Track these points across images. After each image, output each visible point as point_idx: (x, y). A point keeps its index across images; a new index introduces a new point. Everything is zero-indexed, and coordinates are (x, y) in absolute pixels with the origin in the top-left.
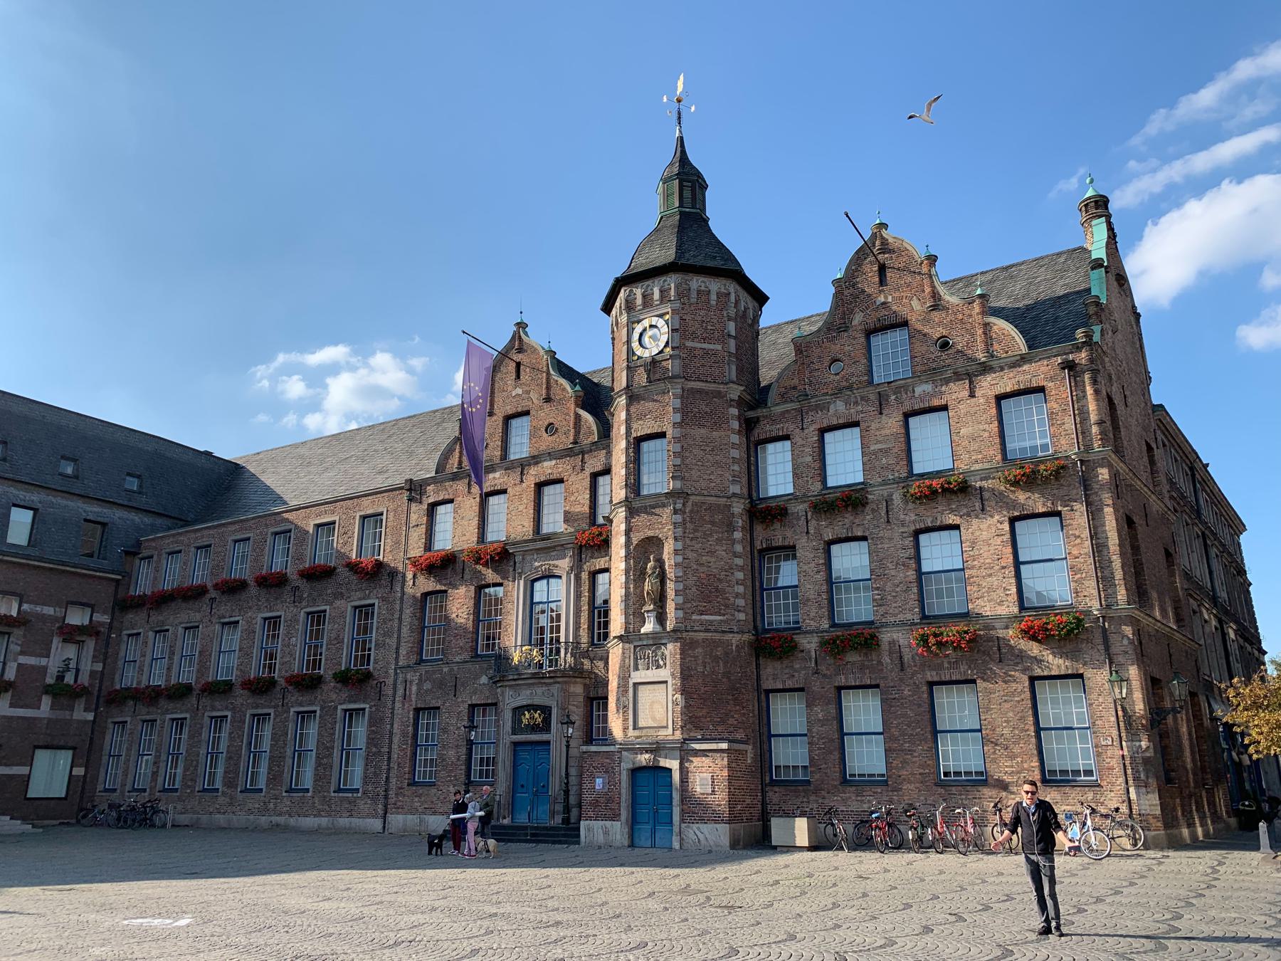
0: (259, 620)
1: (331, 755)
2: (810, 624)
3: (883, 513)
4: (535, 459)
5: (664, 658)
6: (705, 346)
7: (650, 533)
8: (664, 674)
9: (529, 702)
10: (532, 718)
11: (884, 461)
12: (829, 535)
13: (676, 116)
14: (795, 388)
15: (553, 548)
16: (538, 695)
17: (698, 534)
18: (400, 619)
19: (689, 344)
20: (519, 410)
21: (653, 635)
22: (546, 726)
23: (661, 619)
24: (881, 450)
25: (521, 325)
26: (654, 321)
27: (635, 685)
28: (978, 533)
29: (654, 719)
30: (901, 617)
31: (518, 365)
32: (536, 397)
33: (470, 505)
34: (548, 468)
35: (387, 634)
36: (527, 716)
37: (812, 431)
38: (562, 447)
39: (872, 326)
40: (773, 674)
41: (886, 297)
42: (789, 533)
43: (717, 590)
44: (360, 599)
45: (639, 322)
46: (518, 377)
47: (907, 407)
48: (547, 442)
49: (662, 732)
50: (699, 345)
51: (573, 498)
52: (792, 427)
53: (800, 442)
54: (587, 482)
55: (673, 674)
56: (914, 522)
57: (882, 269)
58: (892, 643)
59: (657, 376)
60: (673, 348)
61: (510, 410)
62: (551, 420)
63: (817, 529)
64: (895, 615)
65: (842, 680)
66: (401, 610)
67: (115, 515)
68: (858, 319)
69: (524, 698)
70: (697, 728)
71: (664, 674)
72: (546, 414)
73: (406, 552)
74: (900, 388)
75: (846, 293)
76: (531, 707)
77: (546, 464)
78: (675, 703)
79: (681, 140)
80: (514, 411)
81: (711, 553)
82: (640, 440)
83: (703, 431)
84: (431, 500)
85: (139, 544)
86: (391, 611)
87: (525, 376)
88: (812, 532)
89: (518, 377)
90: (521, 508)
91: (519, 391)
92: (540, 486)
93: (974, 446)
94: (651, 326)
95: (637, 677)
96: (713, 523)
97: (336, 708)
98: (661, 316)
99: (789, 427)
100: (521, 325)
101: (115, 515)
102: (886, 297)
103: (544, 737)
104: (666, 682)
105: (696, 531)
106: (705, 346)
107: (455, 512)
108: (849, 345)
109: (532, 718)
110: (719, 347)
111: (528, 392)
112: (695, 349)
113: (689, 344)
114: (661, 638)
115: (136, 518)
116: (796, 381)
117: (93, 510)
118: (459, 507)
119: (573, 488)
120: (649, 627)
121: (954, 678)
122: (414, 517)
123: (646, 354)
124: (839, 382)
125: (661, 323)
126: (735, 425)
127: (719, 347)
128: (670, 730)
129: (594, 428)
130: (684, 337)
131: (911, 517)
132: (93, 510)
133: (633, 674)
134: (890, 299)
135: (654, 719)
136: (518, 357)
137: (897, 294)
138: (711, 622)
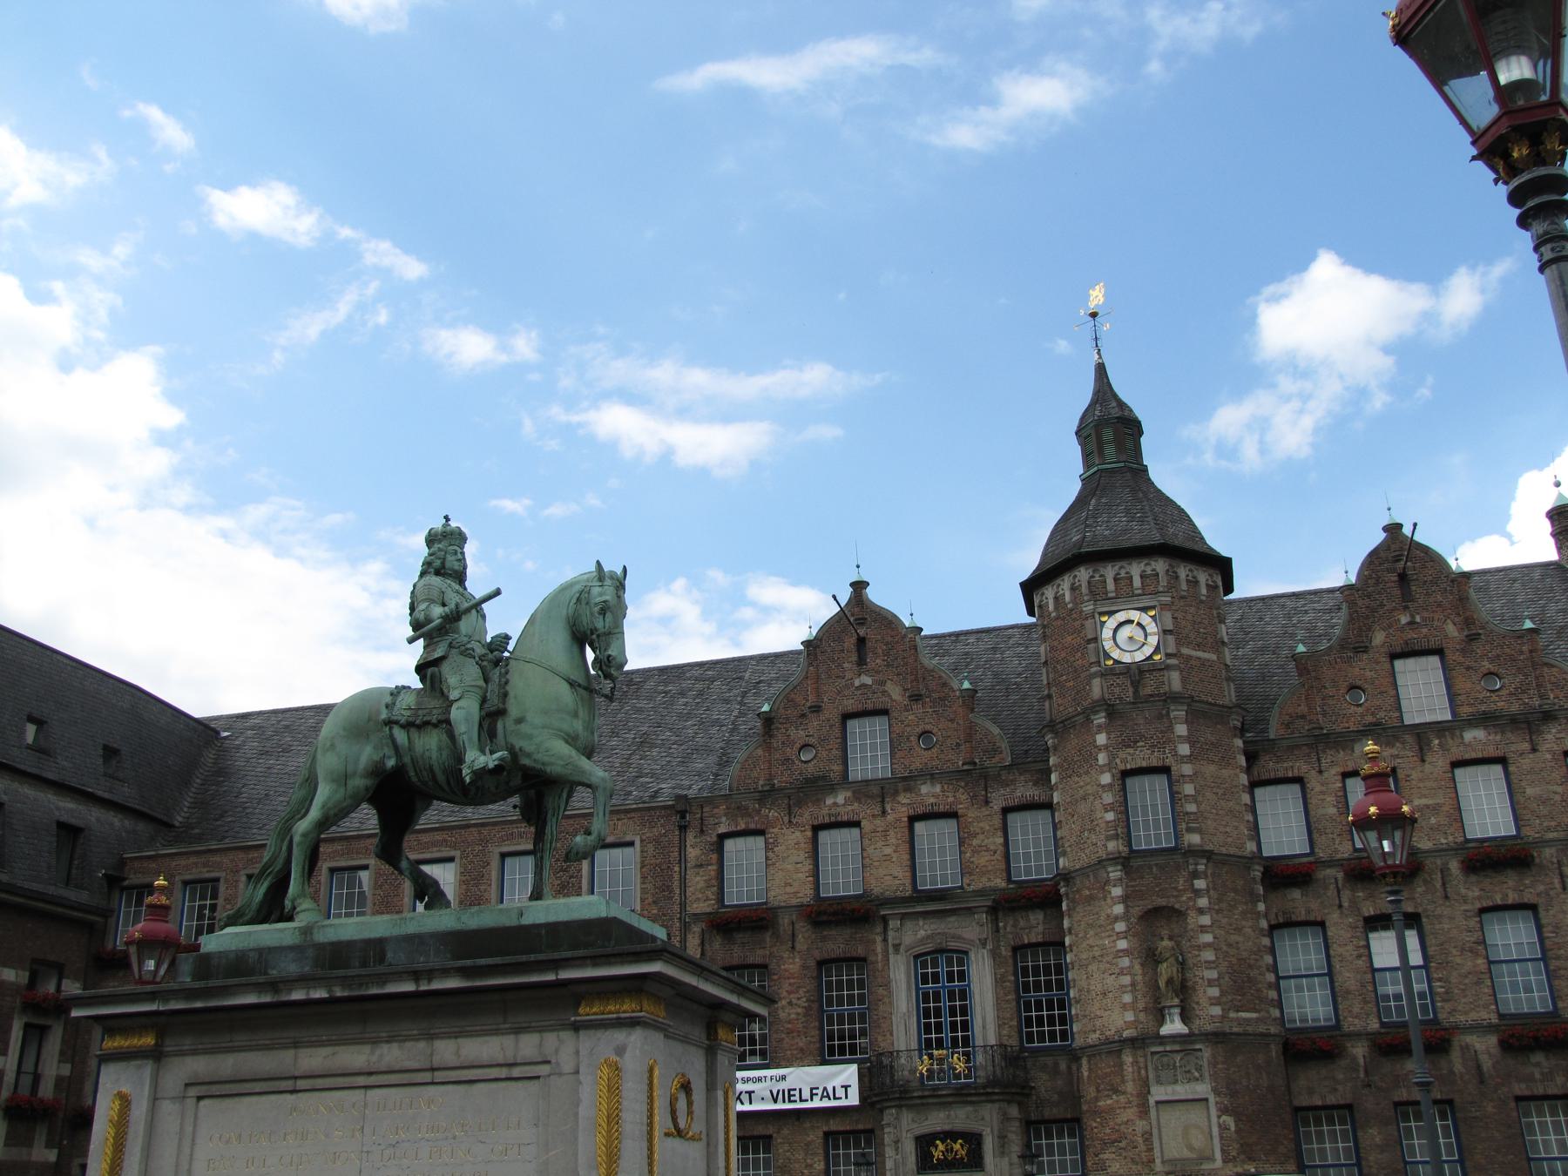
2: (1351, 1024)
3: (1438, 885)
4: (905, 782)
5: (1199, 1069)
6: (1200, 654)
7: (1162, 902)
8: (1202, 1089)
9: (947, 1128)
10: (949, 1150)
11: (1433, 820)
12: (1369, 910)
13: (1090, 335)
14: (1303, 717)
15: (953, 912)
16: (959, 1118)
17: (1224, 905)
19: (1185, 651)
20: (870, 707)
21: (1174, 1038)
23: (1185, 1019)
24: (1427, 806)
25: (859, 586)
26: (1135, 615)
27: (1158, 1103)
28: (1561, 916)
29: (1190, 1148)
30: (1473, 1016)
31: (861, 641)
32: (895, 692)
33: (793, 840)
34: (929, 793)
36: (941, 1147)
37: (1333, 773)
38: (952, 768)
39: (1399, 650)
40: (1316, 1086)
41: (1413, 616)
42: (1314, 905)
43: (1250, 980)
45: (1111, 613)
46: (861, 661)
47: (1457, 753)
48: (921, 758)
49: (1206, 1166)
50: (1194, 653)
51: (975, 842)
52: (1305, 768)
53: (1318, 788)
54: (997, 821)
55: (1215, 1091)
56: (1479, 898)
57: (1403, 578)
58: (1466, 1048)
59: (1148, 691)
60: (1168, 655)
61: (850, 705)
62: (928, 727)
63: (1353, 902)
64: (1466, 1013)
65: (1402, 1094)
67: (90, 816)
68: (1379, 638)
69: (937, 1121)
70: (1251, 1159)
72: (914, 718)
73: (683, 905)
74: (1439, 728)
75: (1360, 603)
77: (924, 789)
78: (1223, 1128)
79: (1101, 370)
80: (860, 707)
81: (1239, 930)
82: (1126, 774)
83: (1212, 768)
84: (722, 829)
85: (122, 863)
87: (875, 661)
88: (1346, 904)
89: (861, 661)
90: (888, 851)
91: (868, 680)
92: (913, 819)
93: (1544, 810)
94: (1139, 624)
96: (1235, 891)
98: (1144, 609)
99: (1300, 767)
100: (859, 586)
101: (90, 816)
102: (1413, 616)
104: (1206, 1100)
105: (1220, 900)
106: (1200, 654)
107: (767, 849)
108: (1362, 669)
109: (949, 1150)
110: (1214, 657)
111: (883, 683)
112: (1190, 657)
113: (1185, 651)
114: (1193, 1042)
115: (116, 820)
116: (1303, 709)
117: (67, 808)
118: (776, 843)
119: (975, 827)
120: (1174, 1026)
121: (1550, 1092)
122: (692, 853)
123: (1127, 658)
124: (1362, 716)
125: (1146, 619)
126: (1242, 761)
127: (1214, 657)
128: (1219, 1163)
129: (1004, 745)
130: (1179, 643)
131: (1473, 892)
132: (67, 808)
133: (1153, 1090)
134: (1418, 619)
135: (1190, 1148)
136: (862, 632)
137: (1426, 614)
138: (1248, 1020)
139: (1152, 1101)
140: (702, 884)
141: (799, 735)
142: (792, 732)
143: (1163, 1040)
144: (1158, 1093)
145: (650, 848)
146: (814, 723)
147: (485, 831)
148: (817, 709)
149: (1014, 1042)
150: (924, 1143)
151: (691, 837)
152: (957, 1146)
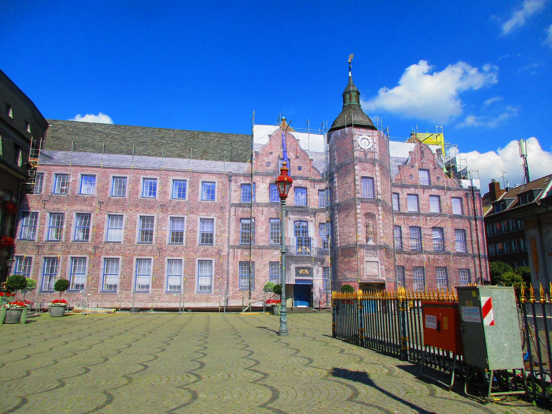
0: (139, 217)
1: (193, 278)
8: (377, 259)
18: (229, 227)
22: (311, 274)
35: (223, 232)
44: (205, 216)
49: (377, 277)
66: (229, 223)
71: (377, 259)
76: (303, 268)
78: (382, 269)
84: (242, 182)
86: (223, 223)
95: (366, 259)
97: (195, 259)
103: (311, 278)
120: (371, 243)
139: (365, 261)
140: (236, 196)
141: (266, 160)
142: (264, 158)
143: (368, 246)
144: (366, 259)
145: (220, 184)
146: (271, 157)
147: (168, 172)
148: (271, 153)
149: (322, 247)
150: (297, 269)
151: (232, 183)
152: (306, 271)
